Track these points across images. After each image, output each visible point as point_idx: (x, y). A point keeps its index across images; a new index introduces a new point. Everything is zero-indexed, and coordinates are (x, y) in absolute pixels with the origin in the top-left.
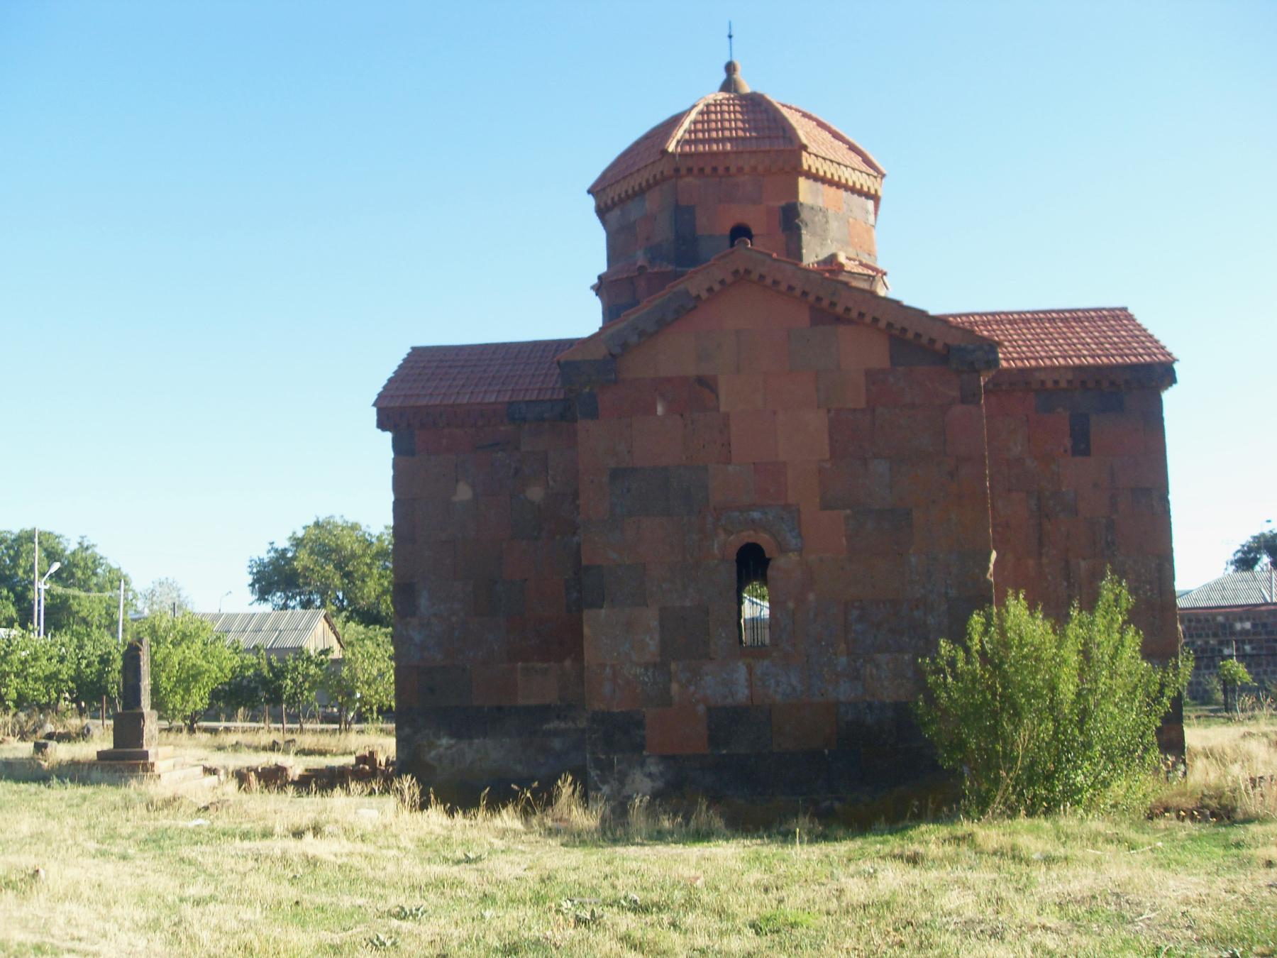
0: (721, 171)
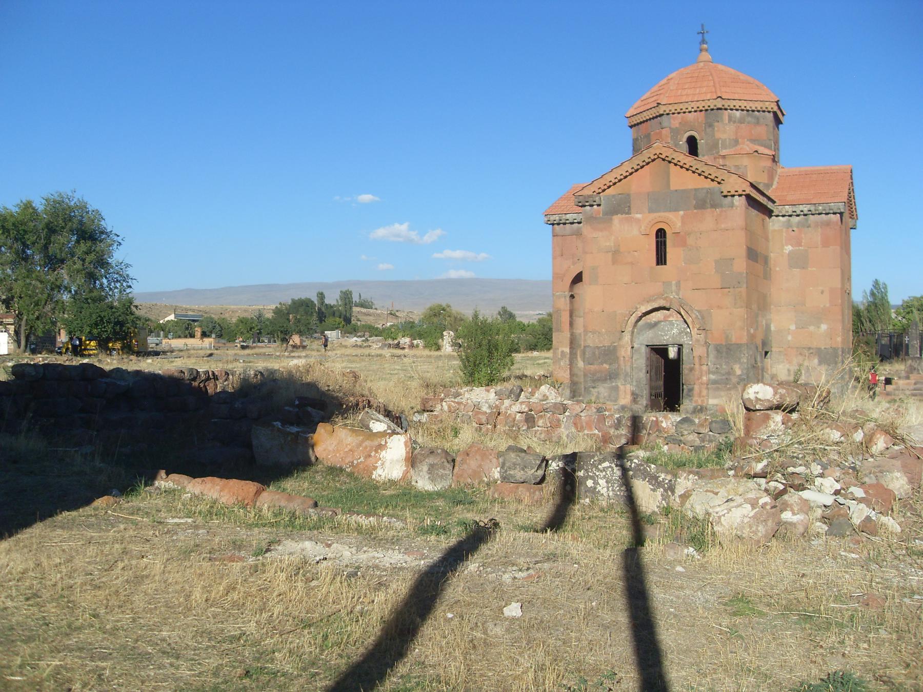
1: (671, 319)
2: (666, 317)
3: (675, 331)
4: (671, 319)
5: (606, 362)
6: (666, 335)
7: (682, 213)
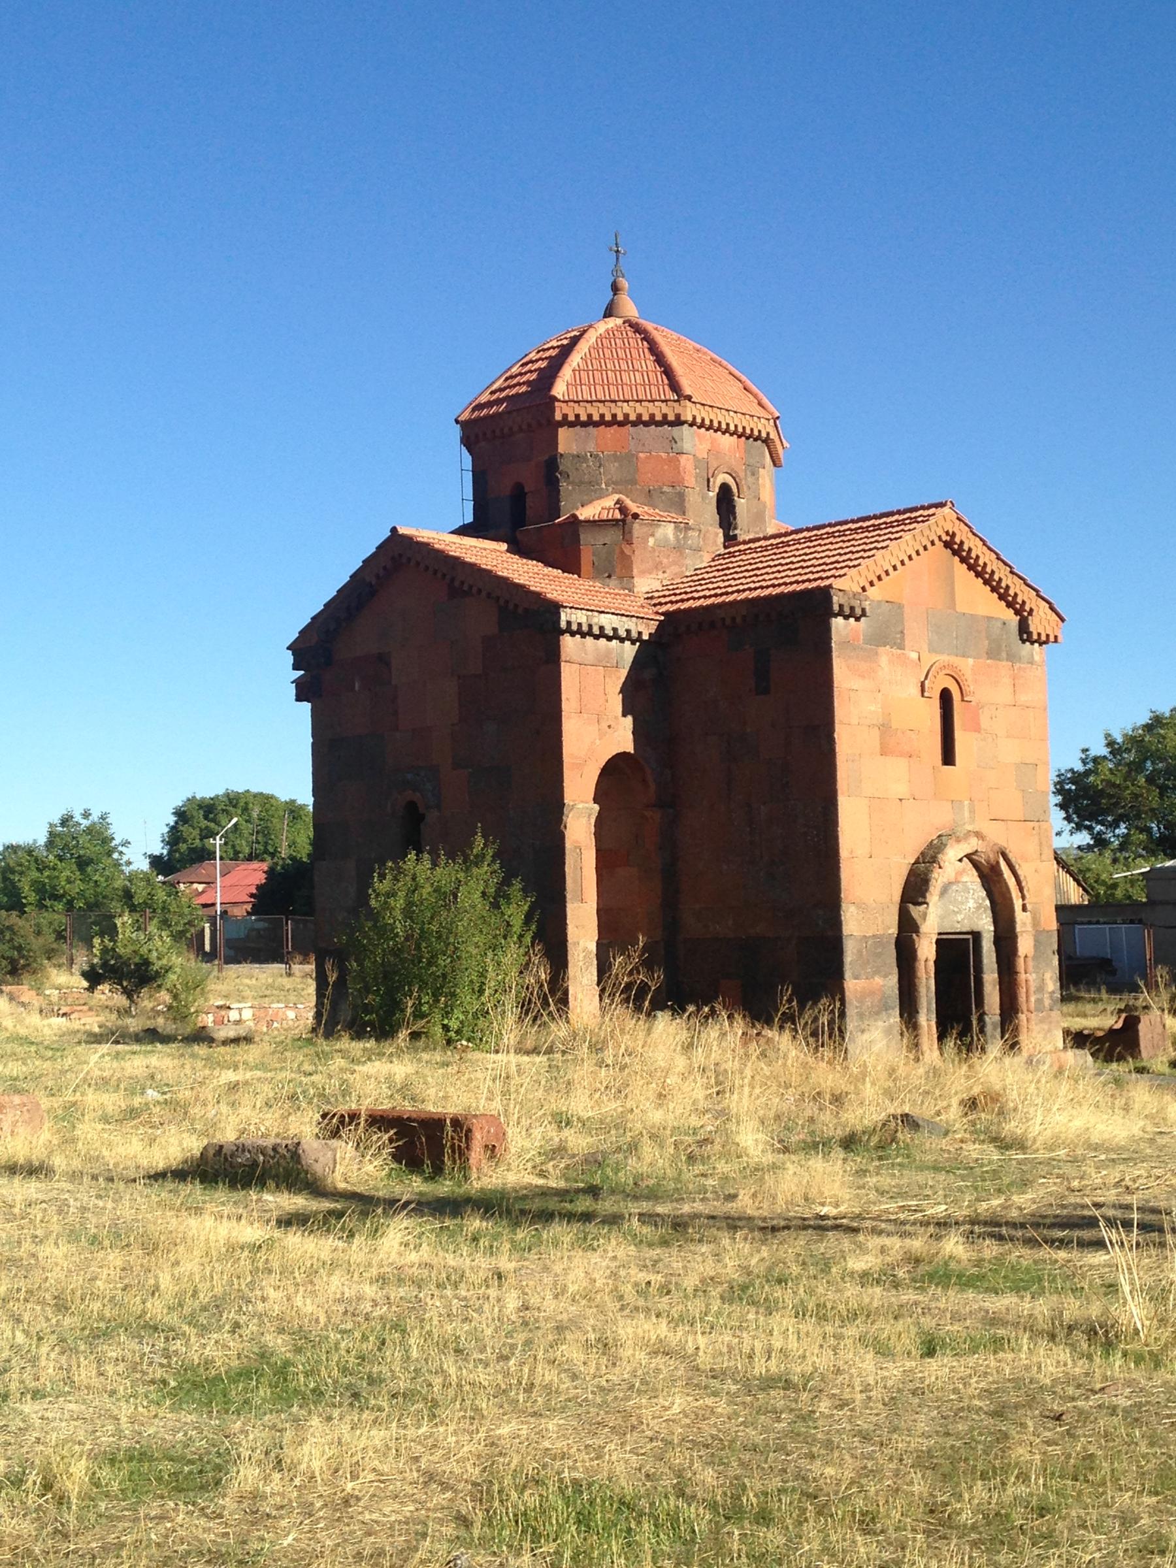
0: (498, 433)
1: (965, 879)
2: (960, 873)
3: (971, 904)
4: (965, 879)
5: (877, 972)
6: (959, 912)
7: (971, 661)
